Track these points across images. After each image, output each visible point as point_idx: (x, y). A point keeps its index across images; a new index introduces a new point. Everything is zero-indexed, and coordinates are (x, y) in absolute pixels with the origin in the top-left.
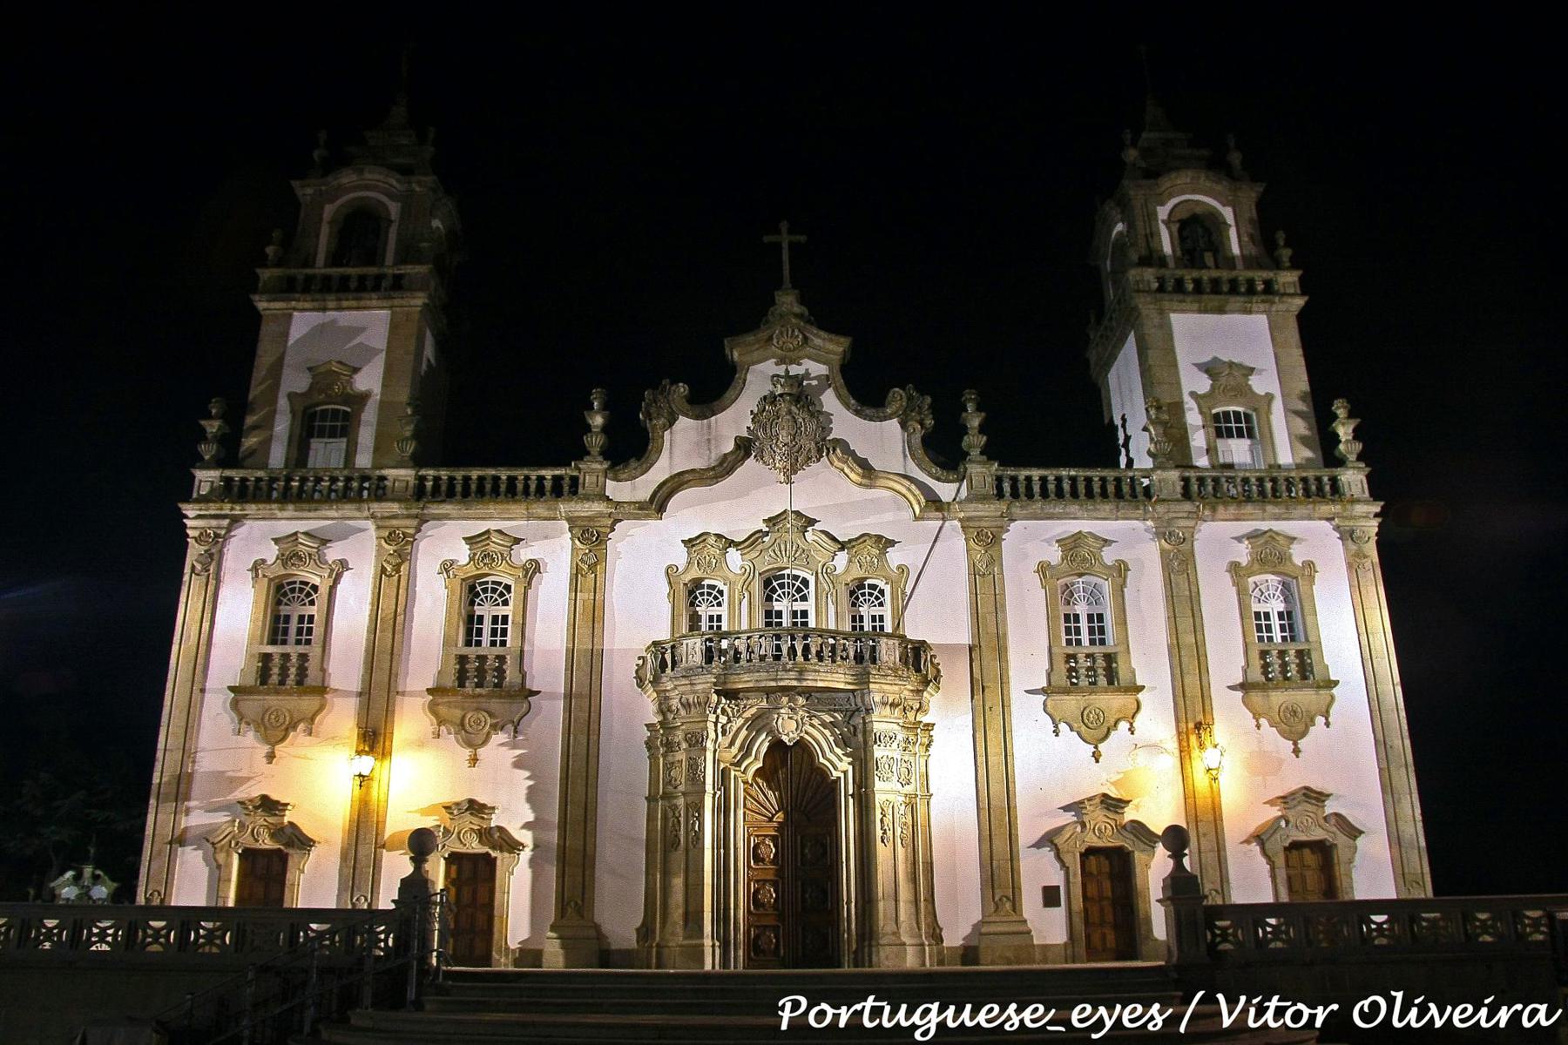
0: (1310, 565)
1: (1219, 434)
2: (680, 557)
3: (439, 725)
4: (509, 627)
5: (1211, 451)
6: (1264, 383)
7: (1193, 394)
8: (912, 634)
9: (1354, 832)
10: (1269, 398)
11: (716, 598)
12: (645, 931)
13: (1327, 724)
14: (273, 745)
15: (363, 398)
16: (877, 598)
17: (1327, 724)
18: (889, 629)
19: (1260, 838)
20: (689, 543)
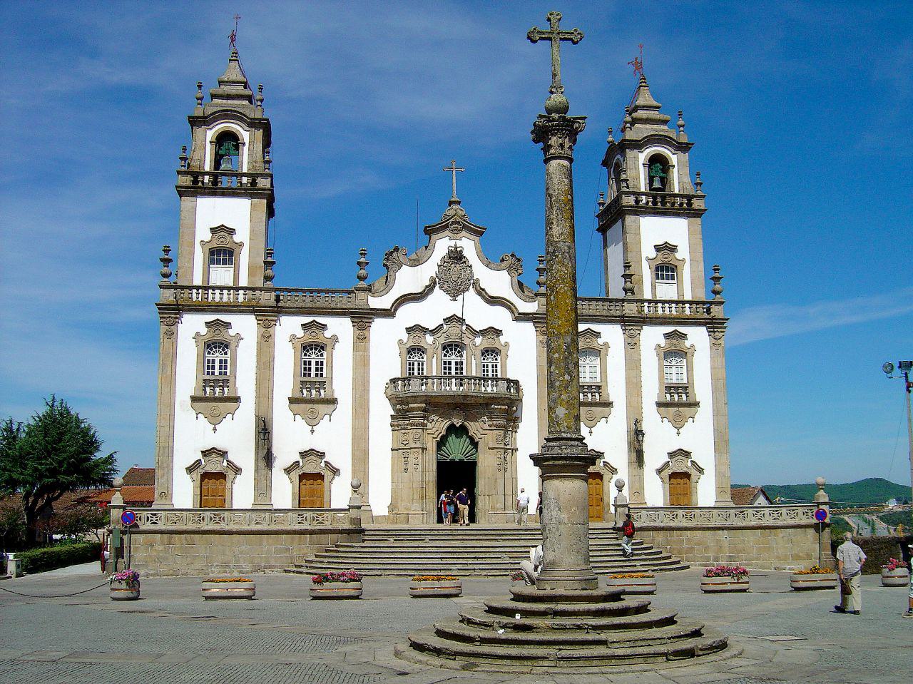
0: (692, 346)
1: (657, 278)
2: (405, 336)
3: (295, 415)
4: (324, 366)
5: (654, 287)
6: (683, 253)
7: (648, 259)
8: (511, 376)
9: (701, 471)
10: (683, 260)
11: (421, 355)
12: (392, 507)
13: (693, 422)
14: (215, 425)
15: (241, 245)
16: (495, 356)
17: (693, 422)
18: (499, 376)
19: (659, 471)
20: (409, 330)
